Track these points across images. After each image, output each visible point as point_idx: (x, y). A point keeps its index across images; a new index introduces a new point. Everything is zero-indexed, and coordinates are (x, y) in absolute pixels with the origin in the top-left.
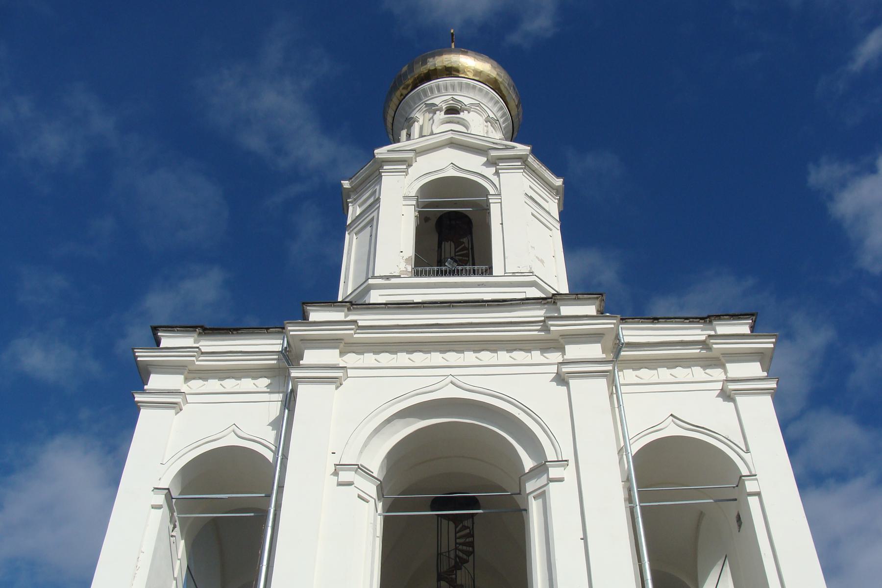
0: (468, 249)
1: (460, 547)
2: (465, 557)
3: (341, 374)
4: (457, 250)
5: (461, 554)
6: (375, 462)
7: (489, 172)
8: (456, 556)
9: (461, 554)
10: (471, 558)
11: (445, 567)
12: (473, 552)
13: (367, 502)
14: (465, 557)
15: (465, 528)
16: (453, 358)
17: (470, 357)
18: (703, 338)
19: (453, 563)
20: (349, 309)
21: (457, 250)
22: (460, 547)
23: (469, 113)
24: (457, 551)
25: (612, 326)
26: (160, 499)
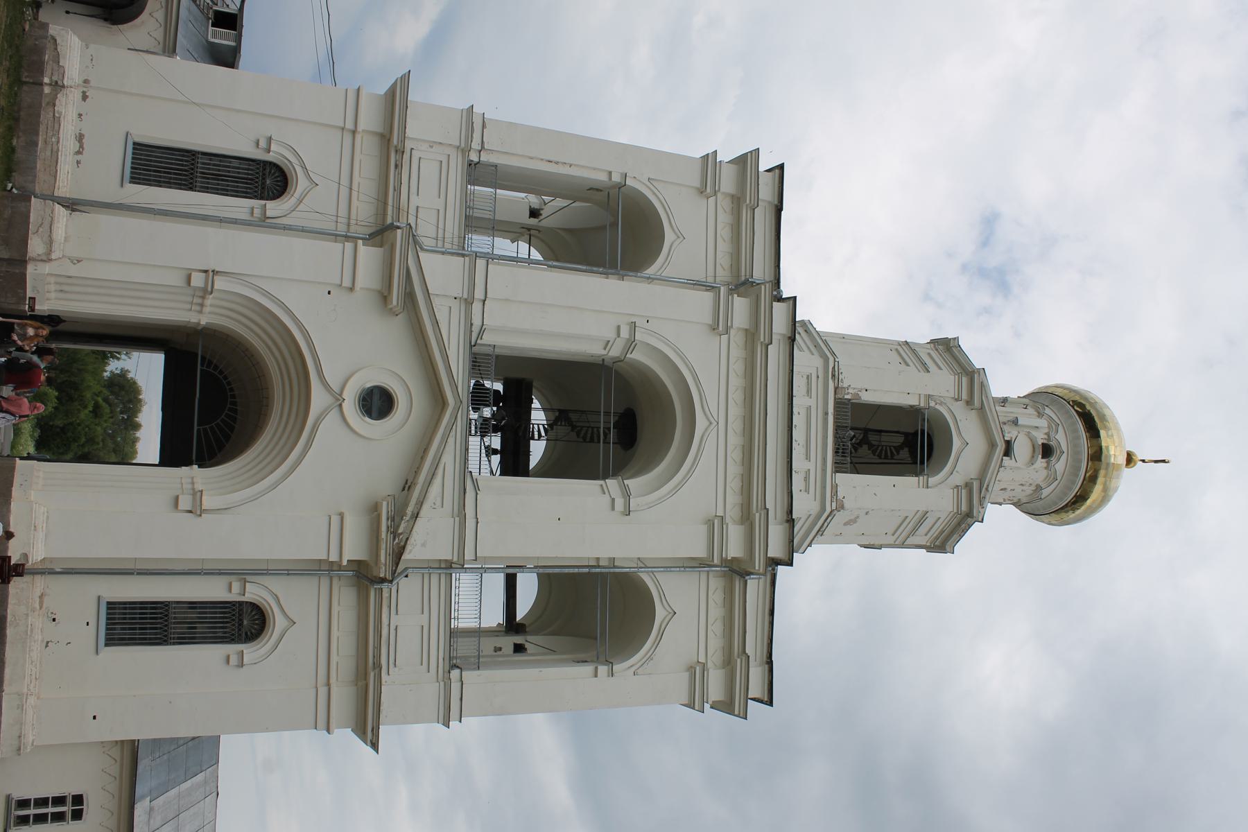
0: (892, 459)
2: (582, 435)
3: (721, 329)
4: (892, 448)
5: (583, 432)
6: (637, 356)
7: (958, 479)
9: (583, 432)
11: (573, 417)
12: (585, 440)
13: (605, 349)
14: (582, 435)
16: (736, 425)
17: (735, 440)
19: (578, 424)
20: (789, 338)
21: (892, 448)
22: (590, 432)
23: (1046, 468)
24: (586, 428)
25: (757, 568)
26: (616, 178)
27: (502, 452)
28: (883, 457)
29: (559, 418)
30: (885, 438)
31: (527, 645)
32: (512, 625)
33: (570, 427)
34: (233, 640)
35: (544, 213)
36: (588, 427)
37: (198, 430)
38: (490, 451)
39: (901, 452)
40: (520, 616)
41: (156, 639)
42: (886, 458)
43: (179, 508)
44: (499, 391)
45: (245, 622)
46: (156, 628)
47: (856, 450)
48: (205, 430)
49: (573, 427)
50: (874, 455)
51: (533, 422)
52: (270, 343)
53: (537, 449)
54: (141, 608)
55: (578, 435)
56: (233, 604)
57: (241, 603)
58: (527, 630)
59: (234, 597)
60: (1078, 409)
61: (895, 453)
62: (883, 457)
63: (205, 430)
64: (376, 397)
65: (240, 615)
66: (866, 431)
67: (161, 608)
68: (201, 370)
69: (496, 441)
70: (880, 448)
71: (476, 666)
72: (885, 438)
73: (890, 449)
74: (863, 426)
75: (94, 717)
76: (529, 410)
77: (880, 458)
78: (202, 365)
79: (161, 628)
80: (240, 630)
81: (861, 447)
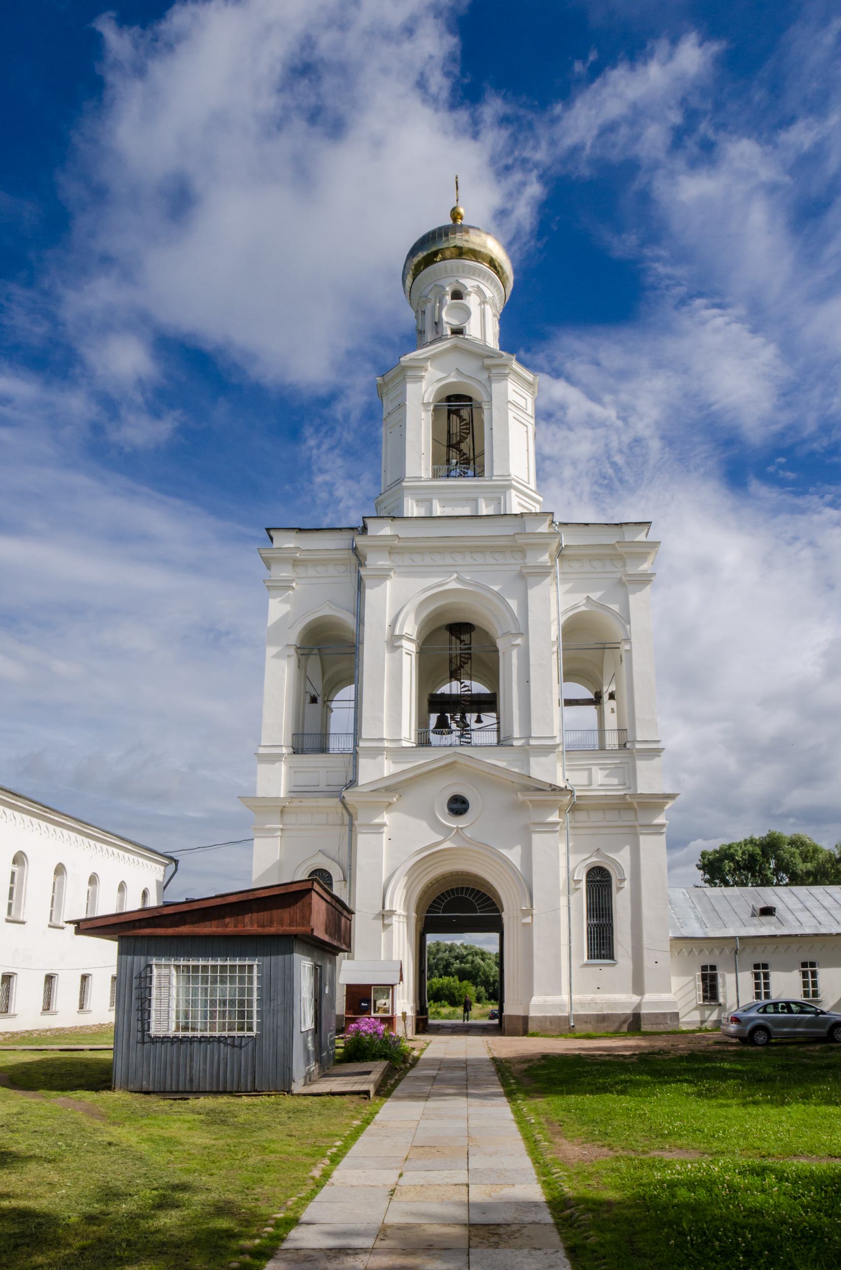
0: (469, 424)
1: (463, 655)
2: (466, 661)
4: (461, 424)
5: (463, 660)
8: (461, 661)
9: (463, 660)
10: (469, 661)
11: (454, 667)
12: (470, 658)
14: (466, 661)
15: (465, 686)
18: (613, 542)
19: (459, 664)
21: (461, 424)
22: (463, 655)
26: (292, 651)
27: (479, 711)
28: (468, 431)
29: (454, 675)
30: (455, 428)
31: (610, 691)
32: (597, 700)
33: (462, 669)
34: (610, 885)
35: (314, 693)
36: (461, 657)
37: (480, 912)
38: (479, 720)
39: (464, 417)
40: (592, 697)
41: (609, 930)
42: (468, 429)
43: (530, 922)
44: (438, 717)
45: (599, 878)
46: (603, 931)
47: (465, 454)
48: (479, 909)
49: (461, 667)
50: (467, 438)
51: (459, 693)
52: (425, 872)
53: (478, 688)
54: (591, 940)
55: (467, 663)
56: (587, 886)
57: (587, 882)
58: (599, 690)
59: (583, 885)
60: (422, 267)
61: (465, 422)
62: (468, 431)
63: (479, 909)
64: (455, 806)
65: (594, 882)
66: (450, 446)
67: (591, 928)
68: (442, 913)
69: (471, 718)
70: (462, 434)
71: (625, 732)
72: (455, 428)
73: (463, 425)
74: (445, 449)
75: (656, 962)
76: (450, 695)
77: (469, 433)
78: (439, 913)
79: (603, 928)
80: (603, 882)
81: (462, 450)
